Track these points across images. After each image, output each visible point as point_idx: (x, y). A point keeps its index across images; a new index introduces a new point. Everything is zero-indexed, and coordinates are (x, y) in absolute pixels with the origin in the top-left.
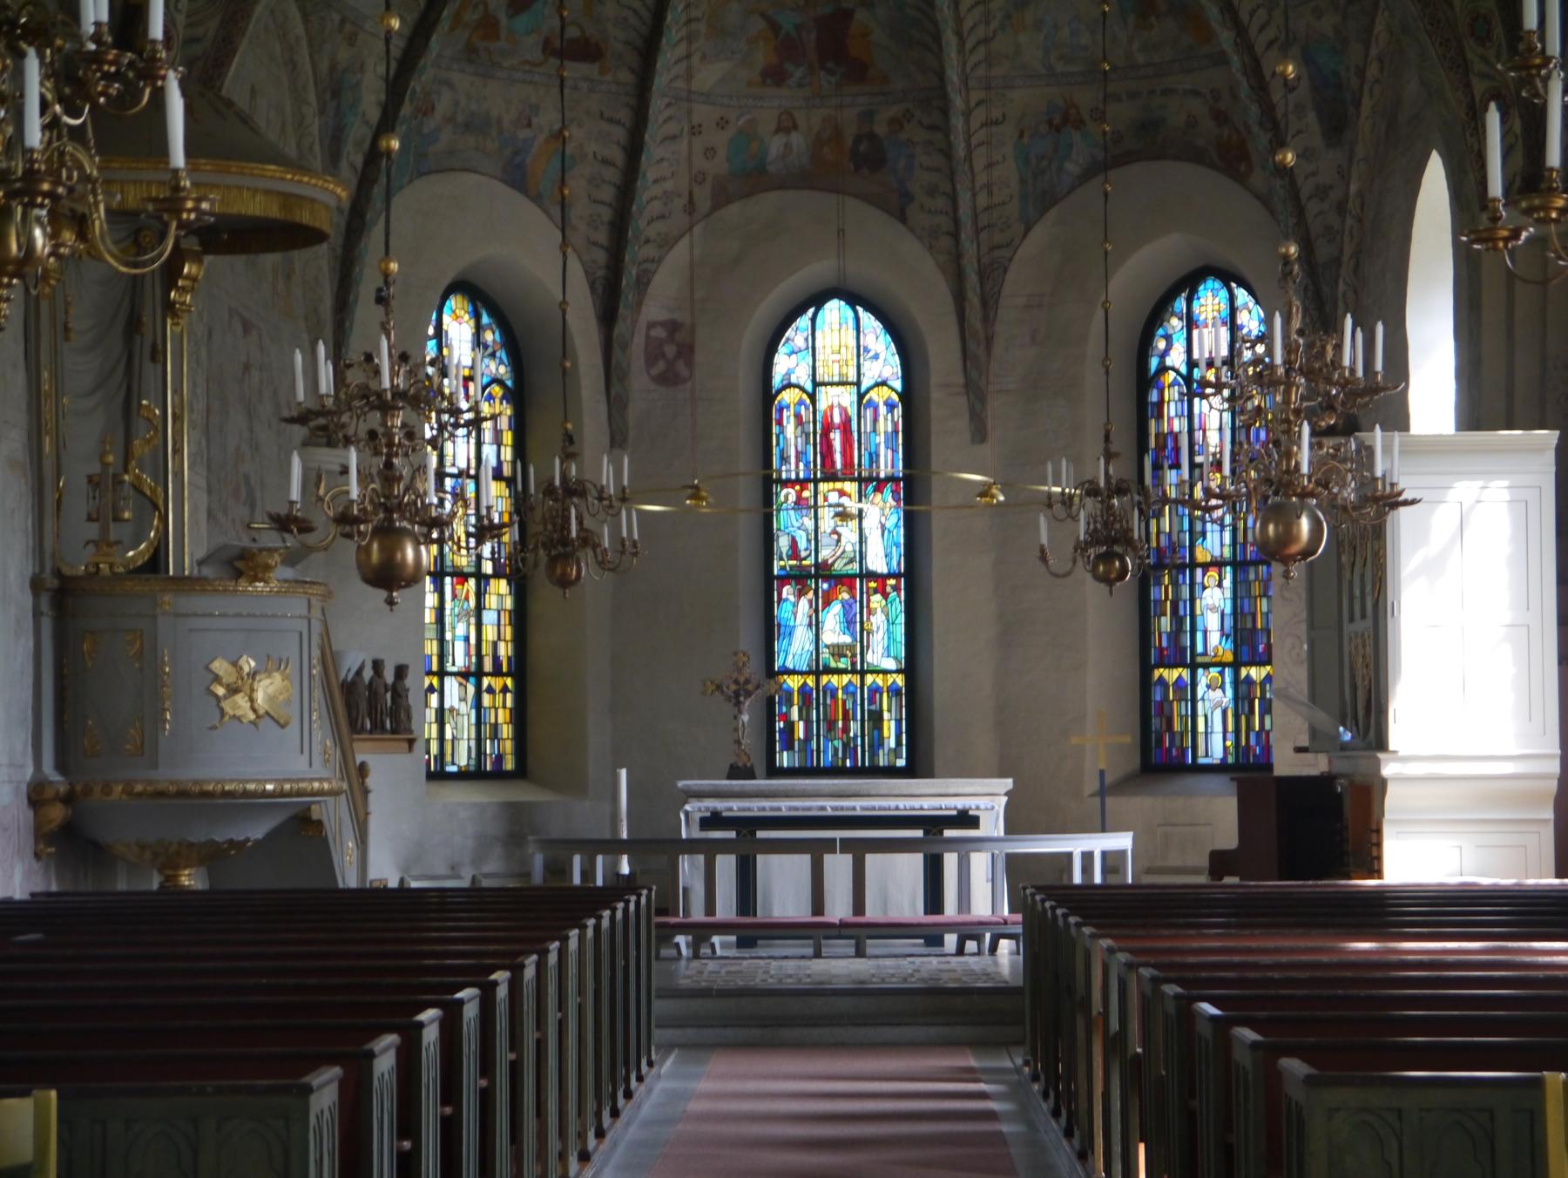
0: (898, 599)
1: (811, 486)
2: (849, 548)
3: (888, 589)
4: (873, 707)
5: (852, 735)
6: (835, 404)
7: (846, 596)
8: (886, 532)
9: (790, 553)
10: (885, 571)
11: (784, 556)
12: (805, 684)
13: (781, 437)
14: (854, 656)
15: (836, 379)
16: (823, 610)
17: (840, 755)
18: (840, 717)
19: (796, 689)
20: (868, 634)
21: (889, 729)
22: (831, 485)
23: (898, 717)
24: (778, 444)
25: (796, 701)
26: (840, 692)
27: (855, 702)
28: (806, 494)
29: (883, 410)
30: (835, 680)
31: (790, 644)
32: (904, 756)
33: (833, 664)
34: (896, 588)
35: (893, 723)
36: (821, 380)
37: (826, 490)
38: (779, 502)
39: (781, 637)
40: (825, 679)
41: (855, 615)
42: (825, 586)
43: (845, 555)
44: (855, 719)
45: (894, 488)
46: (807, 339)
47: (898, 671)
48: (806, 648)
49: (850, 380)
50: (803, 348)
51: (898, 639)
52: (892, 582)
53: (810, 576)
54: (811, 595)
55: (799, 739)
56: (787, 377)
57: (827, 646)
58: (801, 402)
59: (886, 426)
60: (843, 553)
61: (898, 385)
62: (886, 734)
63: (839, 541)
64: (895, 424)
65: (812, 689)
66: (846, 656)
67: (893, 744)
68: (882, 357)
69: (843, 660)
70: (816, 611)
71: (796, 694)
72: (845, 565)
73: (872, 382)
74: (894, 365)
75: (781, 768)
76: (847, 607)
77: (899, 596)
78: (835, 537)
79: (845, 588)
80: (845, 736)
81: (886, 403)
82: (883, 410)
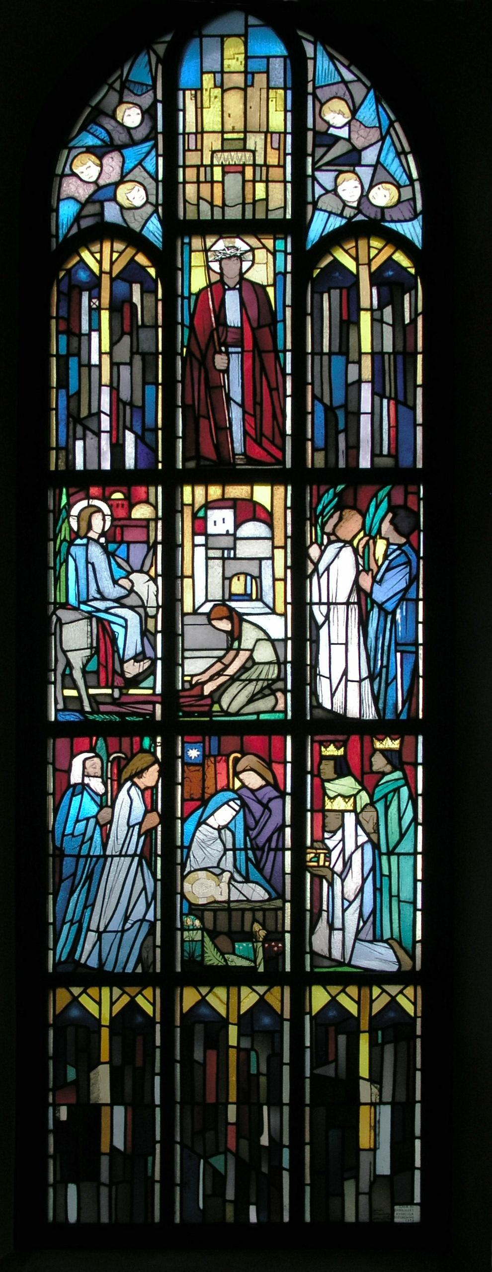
0: (404, 791)
1: (158, 493)
2: (264, 653)
3: (379, 763)
4: (329, 1071)
5: (265, 1140)
6: (231, 280)
7: (253, 780)
8: (375, 614)
9: (92, 666)
10: (370, 714)
11: (78, 675)
12: (132, 1005)
13: (73, 362)
14: (275, 935)
15: (233, 214)
16: (184, 820)
17: (230, 1194)
18: (233, 1097)
19: (105, 1020)
20: (318, 879)
21: (375, 1127)
22: (215, 492)
23: (402, 1097)
24: (63, 383)
25: (105, 1055)
26: (233, 1031)
27: (275, 1058)
28: (141, 512)
29: (368, 295)
30: (218, 998)
31: (89, 905)
32: (417, 1199)
33: (213, 958)
34: (395, 759)
35: (386, 1112)
36: (191, 215)
37: (200, 499)
38: (64, 533)
39: (66, 886)
40: (190, 997)
41: (281, 829)
42: (194, 753)
43: (253, 674)
44: (275, 1101)
45: (398, 500)
46: (149, 113)
47: (400, 978)
48: (137, 914)
49: (276, 215)
50: (138, 135)
51: (407, 894)
52: (391, 744)
53: (149, 727)
54: (151, 777)
55: (113, 1148)
56: (91, 209)
57: (197, 910)
58: (132, 273)
59: (377, 336)
60: (244, 669)
61: (413, 231)
62: (365, 1140)
63: (234, 636)
64: (403, 330)
65: (151, 1021)
66: (250, 937)
67: (384, 1167)
68: (369, 156)
69: (240, 947)
70: (168, 819)
71: (105, 1033)
72: (251, 700)
73: (336, 223)
74: (404, 180)
75: (62, 1224)
76: (257, 809)
77: (409, 782)
78: (225, 625)
79: (249, 760)
80: (244, 1143)
81: (376, 279)
82: (368, 295)
